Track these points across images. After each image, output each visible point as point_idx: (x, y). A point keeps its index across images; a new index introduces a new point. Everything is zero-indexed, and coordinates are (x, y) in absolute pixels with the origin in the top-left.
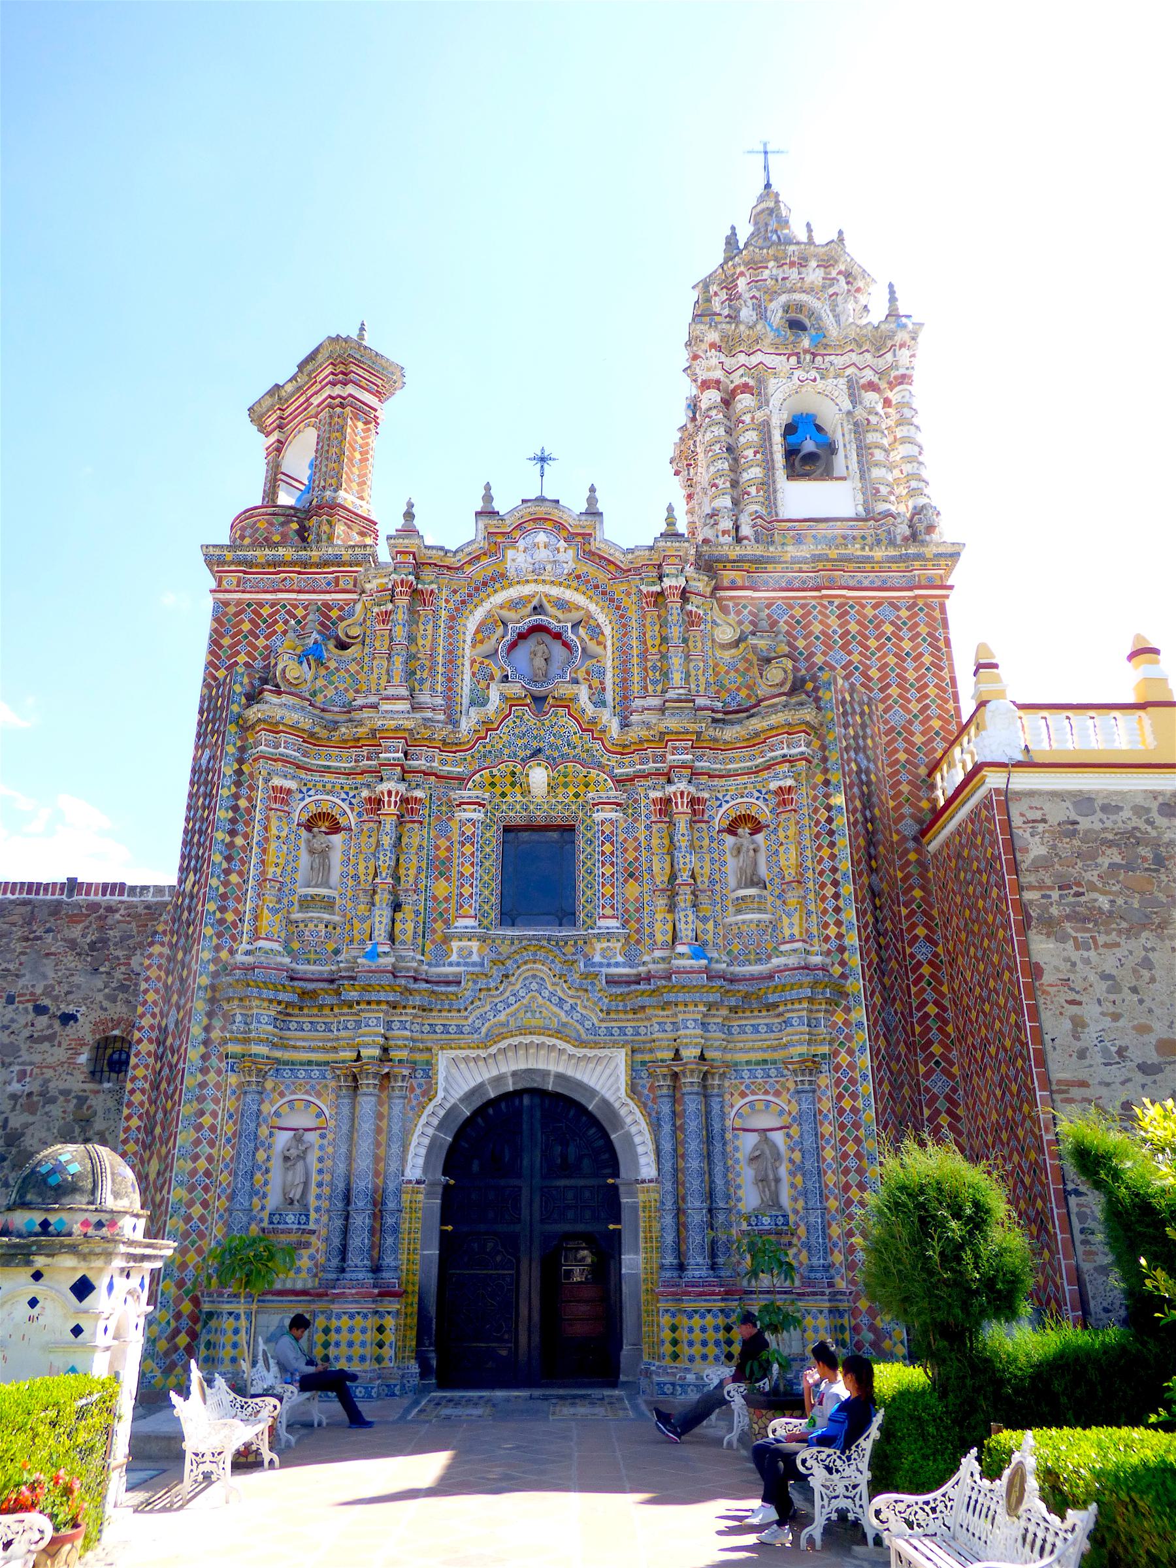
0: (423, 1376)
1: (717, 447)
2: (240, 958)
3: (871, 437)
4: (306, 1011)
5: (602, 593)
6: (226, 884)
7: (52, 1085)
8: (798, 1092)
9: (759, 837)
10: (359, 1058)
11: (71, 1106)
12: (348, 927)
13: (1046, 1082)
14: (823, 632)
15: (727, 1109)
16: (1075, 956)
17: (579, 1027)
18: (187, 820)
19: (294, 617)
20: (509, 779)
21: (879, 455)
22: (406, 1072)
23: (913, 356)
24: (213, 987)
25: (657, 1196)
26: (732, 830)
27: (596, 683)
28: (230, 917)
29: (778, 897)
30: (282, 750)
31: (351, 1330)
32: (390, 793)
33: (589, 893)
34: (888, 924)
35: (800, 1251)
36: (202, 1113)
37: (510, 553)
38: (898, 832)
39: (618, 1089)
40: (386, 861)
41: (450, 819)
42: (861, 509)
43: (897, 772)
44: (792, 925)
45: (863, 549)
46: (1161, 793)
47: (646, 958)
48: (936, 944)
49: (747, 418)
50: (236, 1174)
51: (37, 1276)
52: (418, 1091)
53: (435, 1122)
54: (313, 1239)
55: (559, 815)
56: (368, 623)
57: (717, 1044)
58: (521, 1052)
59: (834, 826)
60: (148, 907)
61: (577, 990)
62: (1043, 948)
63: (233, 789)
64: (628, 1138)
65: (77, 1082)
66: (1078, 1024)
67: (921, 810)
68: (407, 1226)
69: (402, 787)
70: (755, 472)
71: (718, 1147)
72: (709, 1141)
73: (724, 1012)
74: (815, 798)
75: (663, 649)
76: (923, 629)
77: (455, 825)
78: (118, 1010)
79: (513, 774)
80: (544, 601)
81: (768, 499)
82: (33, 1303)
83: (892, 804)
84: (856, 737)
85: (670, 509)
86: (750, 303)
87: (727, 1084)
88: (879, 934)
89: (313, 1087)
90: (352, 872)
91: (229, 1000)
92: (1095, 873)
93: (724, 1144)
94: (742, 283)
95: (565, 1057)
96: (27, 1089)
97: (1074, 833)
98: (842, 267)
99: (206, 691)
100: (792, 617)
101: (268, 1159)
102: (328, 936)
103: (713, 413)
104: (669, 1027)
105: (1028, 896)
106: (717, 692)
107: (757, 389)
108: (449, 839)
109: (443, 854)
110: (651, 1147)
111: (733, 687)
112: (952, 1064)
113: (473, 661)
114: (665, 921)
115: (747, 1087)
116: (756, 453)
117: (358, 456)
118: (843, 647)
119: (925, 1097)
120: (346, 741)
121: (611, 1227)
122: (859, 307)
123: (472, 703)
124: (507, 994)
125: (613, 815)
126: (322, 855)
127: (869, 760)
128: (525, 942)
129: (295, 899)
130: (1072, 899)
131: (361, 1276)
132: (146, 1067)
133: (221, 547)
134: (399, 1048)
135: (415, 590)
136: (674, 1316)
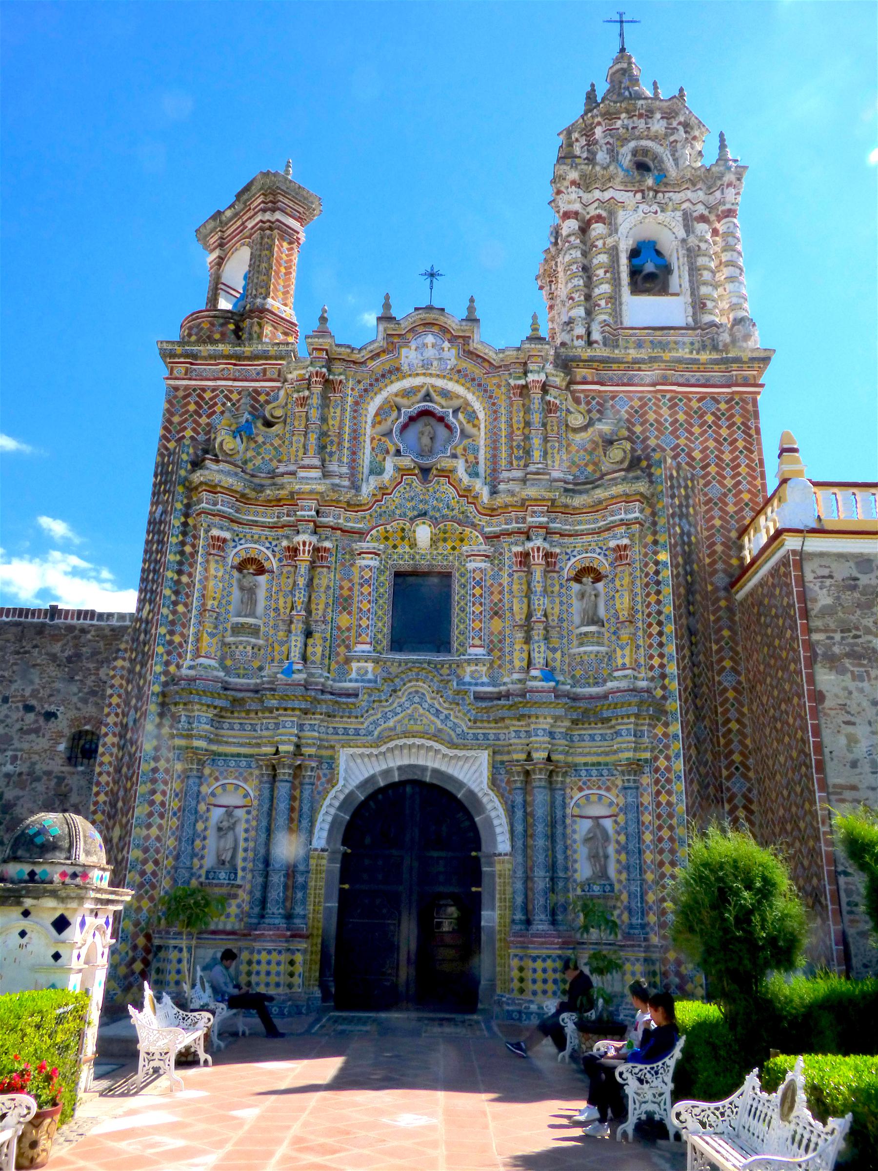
0: (324, 999)
1: (574, 267)
2: (184, 672)
3: (701, 261)
4: (236, 714)
5: (479, 386)
6: (174, 612)
7: (37, 767)
8: (625, 788)
9: (600, 585)
10: (277, 752)
11: (53, 783)
12: (270, 649)
13: (823, 786)
14: (656, 420)
15: (568, 801)
16: (852, 685)
17: (452, 733)
18: (144, 561)
19: (230, 400)
21: (707, 275)
22: (314, 764)
23: (738, 194)
24: (164, 694)
25: (510, 866)
26: (577, 578)
27: (471, 458)
28: (177, 639)
29: (614, 633)
30: (219, 507)
31: (269, 963)
32: (304, 544)
33: (462, 626)
35: (622, 912)
36: (153, 792)
37: (404, 351)
38: (712, 584)
39: (482, 782)
40: (300, 597)
41: (352, 565)
42: (690, 320)
43: (713, 535)
44: (623, 656)
45: (691, 352)
47: (506, 680)
49: (600, 243)
50: (180, 841)
51: (26, 914)
52: (323, 780)
53: (337, 804)
54: (240, 892)
55: (440, 564)
56: (289, 406)
57: (561, 749)
58: (405, 751)
59: (660, 578)
60: (113, 629)
61: (451, 703)
62: (826, 679)
63: (181, 538)
64: (489, 822)
65: (58, 766)
66: (852, 740)
67: (731, 565)
68: (313, 883)
69: (314, 539)
70: (605, 288)
71: (559, 829)
72: (553, 825)
73: (567, 723)
74: (646, 555)
75: (526, 431)
76: (738, 420)
77: (355, 570)
78: (90, 710)
79: (403, 530)
81: (615, 310)
82: (23, 934)
83: (707, 561)
84: (680, 506)
85: (535, 317)
86: (605, 148)
87: (568, 780)
89: (241, 774)
90: (274, 606)
91: (176, 704)
92: (871, 620)
93: (565, 828)
94: (599, 131)
95: (440, 756)
96: (18, 770)
97: (854, 588)
98: (682, 119)
99: (159, 459)
100: (632, 407)
101: (206, 829)
102: (254, 655)
103: (572, 239)
104: (523, 735)
105: (815, 637)
106: (569, 467)
107: (609, 219)
108: (350, 581)
109: (346, 593)
110: (506, 828)
111: (582, 463)
113: (373, 439)
114: (522, 650)
115: (584, 783)
116: (606, 272)
118: (672, 433)
119: (726, 795)
120: (270, 501)
121: (474, 889)
122: (694, 153)
123: (371, 472)
124: (395, 705)
125: (483, 565)
126: (250, 592)
127: (690, 525)
128: (410, 665)
129: (229, 626)
130: (851, 641)
131: (277, 921)
132: (111, 755)
133: (173, 343)
134: (308, 745)
135: (327, 381)
136: (521, 959)
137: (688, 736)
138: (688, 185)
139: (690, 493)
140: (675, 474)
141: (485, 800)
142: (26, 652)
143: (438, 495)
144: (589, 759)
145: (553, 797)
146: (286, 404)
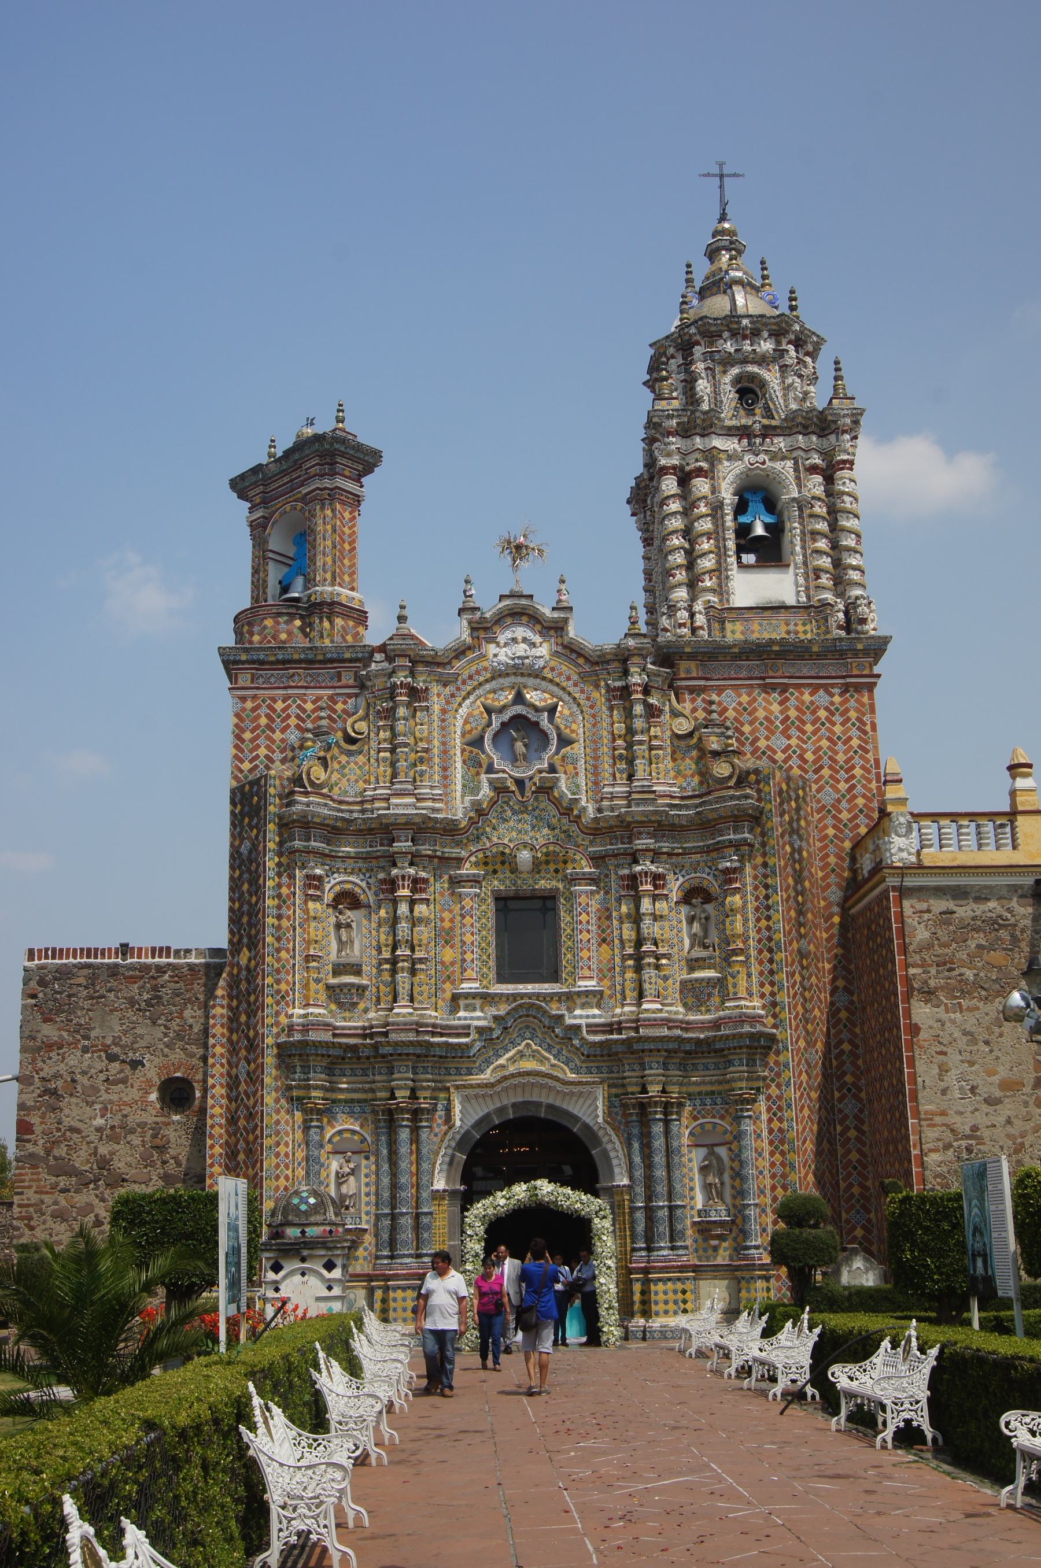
6: (279, 960)
13: (916, 1114)
14: (766, 718)
28: (283, 987)
34: (813, 979)
36: (278, 1144)
38: (824, 899)
39: (597, 1116)
43: (826, 846)
46: (1021, 887)
48: (852, 993)
59: (770, 902)
62: (922, 1012)
64: (605, 1154)
76: (853, 714)
79: (503, 853)
83: (820, 874)
84: (790, 823)
88: (805, 989)
94: (698, 351)
96: (110, 1123)
98: (792, 337)
100: (740, 704)
105: (912, 971)
109: (447, 924)
112: (861, 1091)
113: (463, 751)
115: (699, 1112)
117: (347, 546)
118: (783, 732)
127: (801, 839)
132: (221, 1107)
137: (798, 1064)
138: (800, 428)
139: (803, 805)
140: (784, 787)
141: (601, 1133)
142: (104, 997)
143: (537, 813)
146: (367, 715)
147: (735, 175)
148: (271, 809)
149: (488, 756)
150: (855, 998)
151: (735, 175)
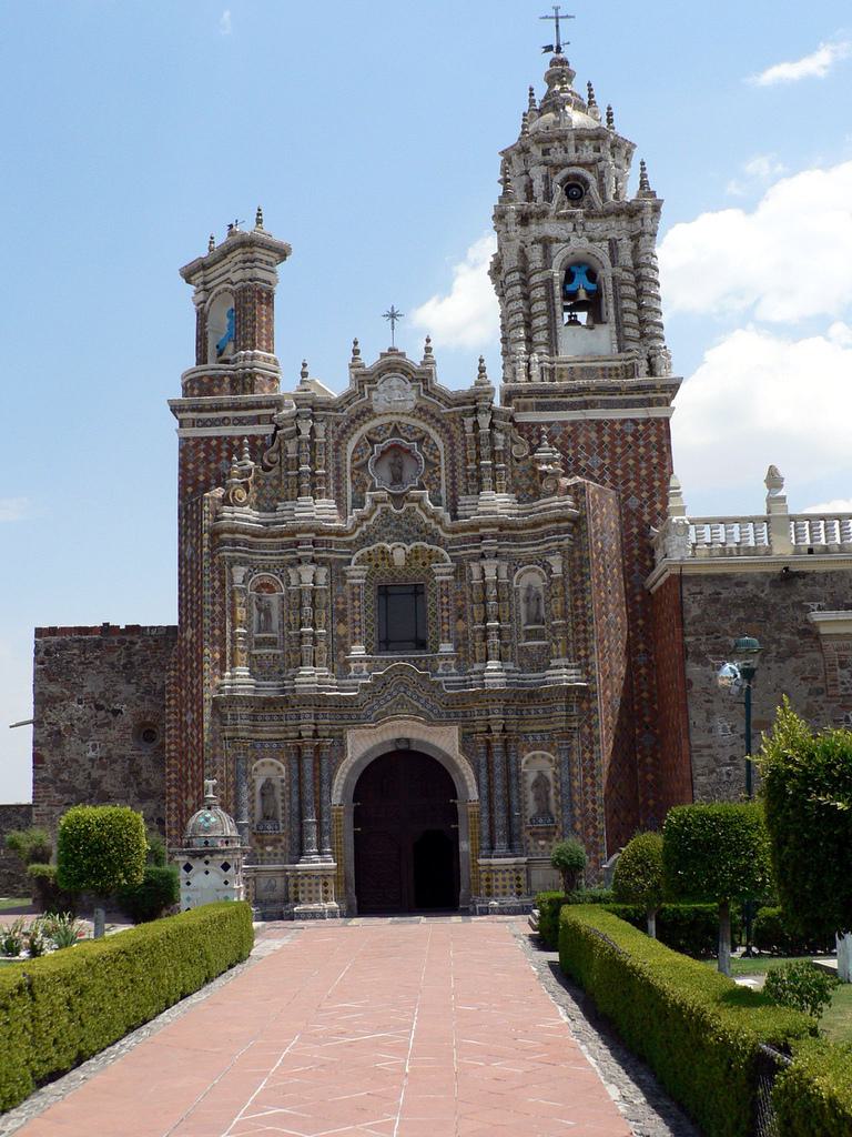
10: (300, 737)
14: (586, 444)
20: (380, 556)
31: (310, 885)
71: (514, 781)
78: (146, 706)
80: (399, 427)
96: (99, 755)
100: (565, 432)
105: (688, 639)
108: (343, 596)
109: (341, 607)
113: (352, 474)
117: (264, 319)
123: (353, 507)
134: (323, 730)
141: (458, 761)
144: (535, 728)
145: (508, 757)
147: (567, 17)
148: (206, 522)
149: (371, 478)
150: (653, 657)
151: (567, 17)
